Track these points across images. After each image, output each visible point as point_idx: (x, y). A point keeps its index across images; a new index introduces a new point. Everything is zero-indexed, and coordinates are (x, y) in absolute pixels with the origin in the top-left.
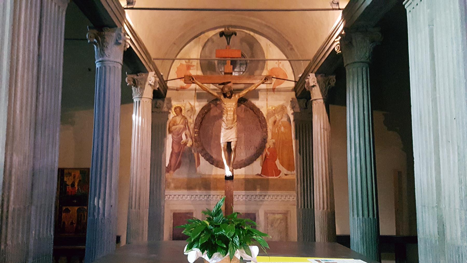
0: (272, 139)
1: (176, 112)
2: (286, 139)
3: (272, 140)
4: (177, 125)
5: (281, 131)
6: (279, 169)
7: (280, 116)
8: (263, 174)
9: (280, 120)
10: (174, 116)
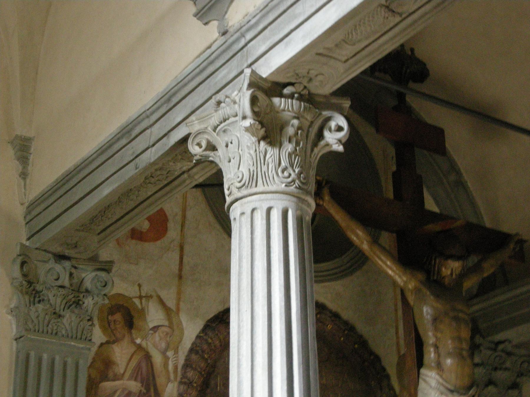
1: (112, 326)
4: (116, 378)
10: (104, 339)
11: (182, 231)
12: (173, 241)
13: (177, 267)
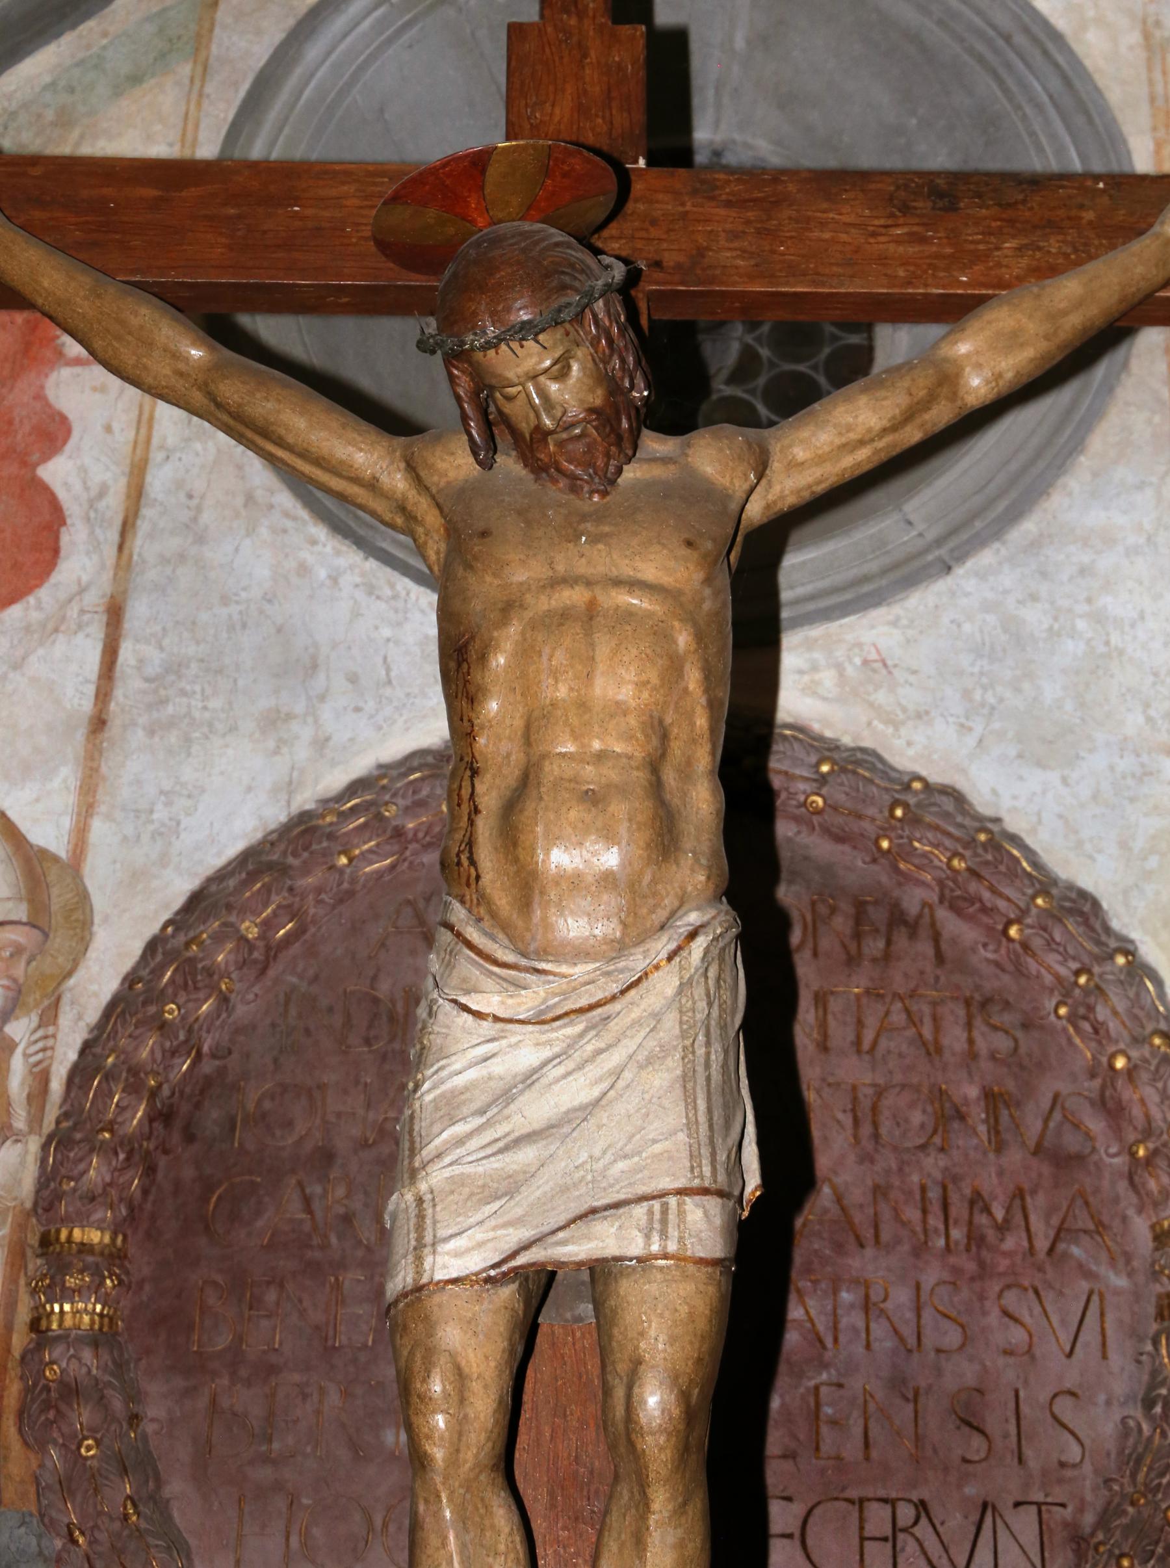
11: (121, 548)
12: (82, 590)
13: (91, 690)
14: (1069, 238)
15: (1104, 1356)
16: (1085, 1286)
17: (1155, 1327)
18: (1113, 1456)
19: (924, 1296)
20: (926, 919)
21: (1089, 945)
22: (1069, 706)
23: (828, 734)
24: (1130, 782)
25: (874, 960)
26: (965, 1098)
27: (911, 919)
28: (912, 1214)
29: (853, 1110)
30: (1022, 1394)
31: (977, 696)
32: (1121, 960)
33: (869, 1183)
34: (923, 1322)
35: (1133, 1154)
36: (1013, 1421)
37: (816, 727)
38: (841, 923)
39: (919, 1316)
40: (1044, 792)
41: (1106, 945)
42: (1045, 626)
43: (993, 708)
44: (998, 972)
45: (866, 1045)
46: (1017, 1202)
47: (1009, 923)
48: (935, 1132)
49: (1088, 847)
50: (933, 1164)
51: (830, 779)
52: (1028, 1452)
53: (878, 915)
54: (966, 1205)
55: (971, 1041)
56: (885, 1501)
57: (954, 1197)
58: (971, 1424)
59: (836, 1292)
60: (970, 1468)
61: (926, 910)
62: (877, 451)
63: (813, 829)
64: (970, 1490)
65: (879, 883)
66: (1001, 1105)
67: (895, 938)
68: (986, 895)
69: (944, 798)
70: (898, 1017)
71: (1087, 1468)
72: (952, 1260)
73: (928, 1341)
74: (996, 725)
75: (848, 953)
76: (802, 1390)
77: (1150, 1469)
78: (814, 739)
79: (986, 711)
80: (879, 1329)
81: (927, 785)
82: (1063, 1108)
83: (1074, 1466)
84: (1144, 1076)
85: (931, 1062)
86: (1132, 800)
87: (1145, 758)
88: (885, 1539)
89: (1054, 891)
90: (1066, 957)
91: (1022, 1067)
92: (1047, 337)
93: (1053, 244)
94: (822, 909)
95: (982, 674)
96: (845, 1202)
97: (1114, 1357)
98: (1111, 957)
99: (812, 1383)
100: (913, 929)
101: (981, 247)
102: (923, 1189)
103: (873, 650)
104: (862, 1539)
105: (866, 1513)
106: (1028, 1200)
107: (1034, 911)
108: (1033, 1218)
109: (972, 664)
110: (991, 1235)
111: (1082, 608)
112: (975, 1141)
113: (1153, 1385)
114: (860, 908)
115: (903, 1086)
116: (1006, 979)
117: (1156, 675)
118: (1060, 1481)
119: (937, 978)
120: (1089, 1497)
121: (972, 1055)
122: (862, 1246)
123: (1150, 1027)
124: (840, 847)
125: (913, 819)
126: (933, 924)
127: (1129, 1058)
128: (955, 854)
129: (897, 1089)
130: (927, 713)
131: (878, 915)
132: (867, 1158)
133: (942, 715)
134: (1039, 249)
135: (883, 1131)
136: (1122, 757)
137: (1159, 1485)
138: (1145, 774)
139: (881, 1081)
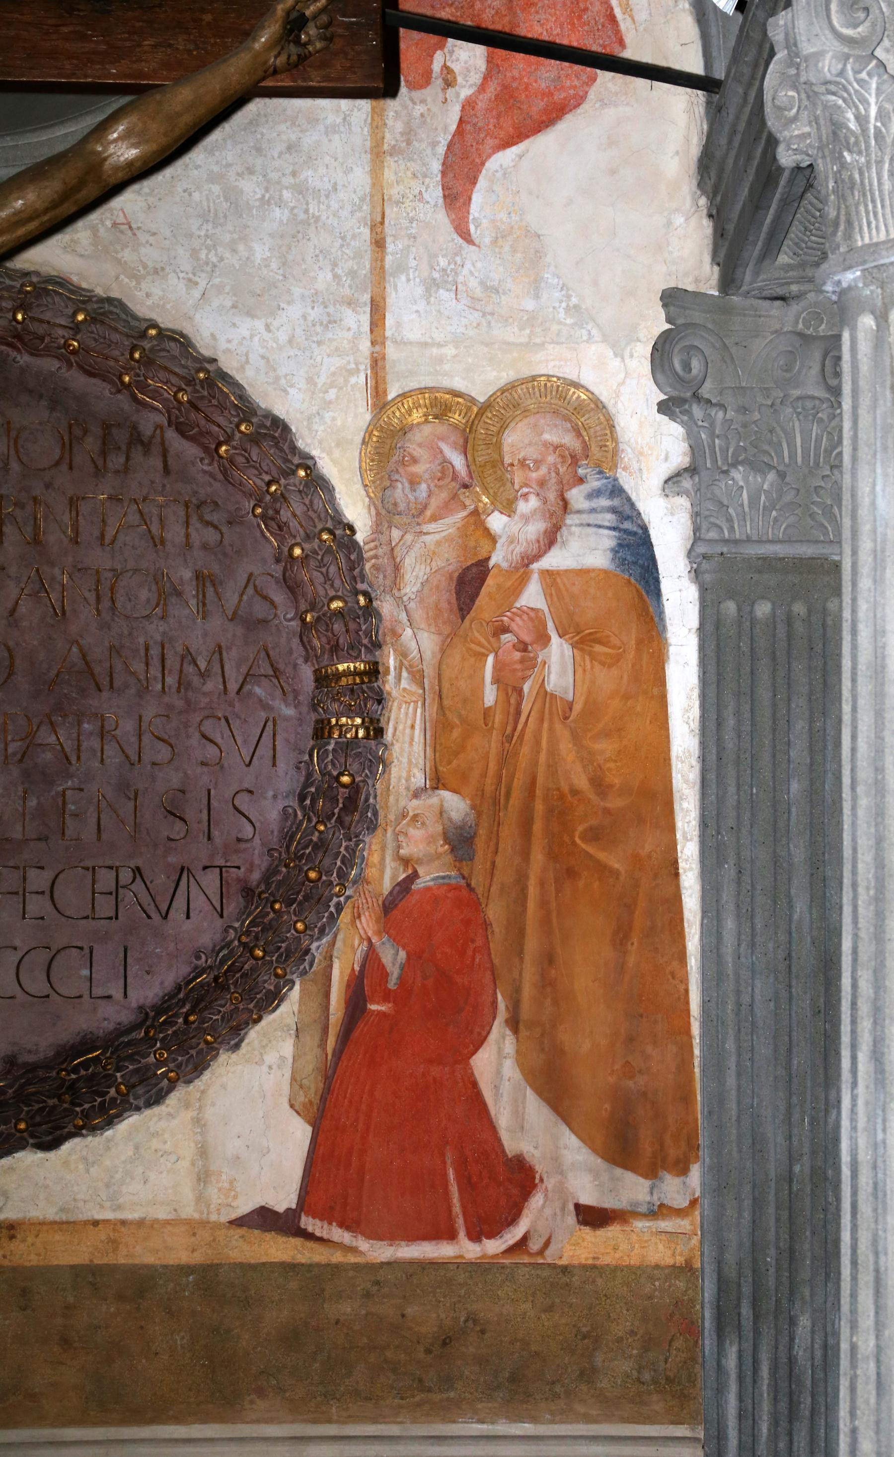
0: (437, 782)
2: (599, 784)
3: (433, 800)
5: (543, 694)
6: (511, 1144)
7: (528, 505)
8: (327, 1215)
9: (529, 559)
14: (192, 37)
15: (274, 765)
16: (263, 715)
17: (312, 743)
18: (276, 833)
19: (144, 725)
20: (158, 439)
21: (279, 462)
22: (274, 266)
23: (84, 285)
24: (318, 329)
25: (117, 472)
26: (181, 578)
27: (145, 439)
28: (138, 666)
29: (97, 590)
30: (212, 792)
31: (203, 256)
32: (302, 473)
33: (107, 644)
34: (143, 744)
35: (303, 621)
36: (205, 812)
37: (75, 279)
38: (91, 444)
39: (140, 740)
40: (252, 336)
41: (291, 462)
42: (259, 196)
43: (215, 266)
44: (212, 480)
45: (107, 540)
46: (217, 656)
47: (219, 444)
48: (157, 605)
49: (283, 381)
50: (155, 630)
51: (82, 327)
52: (215, 833)
53: (121, 436)
54: (178, 659)
55: (187, 536)
56: (111, 868)
57: (169, 654)
58: (174, 814)
59: (79, 724)
60: (173, 844)
61: (158, 431)
62: (42, 224)
63: (72, 365)
64: (172, 859)
65: (122, 410)
66: (208, 584)
67: (133, 455)
68: (203, 422)
69: (172, 344)
70: (133, 518)
71: (257, 841)
72: (166, 699)
73: (146, 758)
74: (217, 281)
75: (96, 467)
76: (53, 793)
77: (299, 843)
78: (72, 292)
79: (209, 269)
80: (111, 750)
81: (160, 330)
82: (255, 586)
83: (247, 841)
84: (313, 563)
85: (156, 552)
86: (319, 343)
87: (331, 309)
88: (111, 893)
89: (254, 420)
90: (260, 471)
91: (225, 555)
92: (165, 135)
93: (180, 43)
94: (77, 432)
95: (207, 236)
96: (88, 658)
97: (281, 765)
98: (294, 473)
99: (60, 789)
100: (147, 447)
101: (128, 44)
102: (147, 649)
103: (121, 214)
104: (94, 893)
105: (97, 876)
106: (224, 654)
107: (238, 435)
108: (227, 668)
109: (200, 229)
110: (196, 681)
111: (288, 180)
112: (187, 611)
113: (306, 785)
114: (107, 428)
115: (136, 571)
116: (217, 485)
117: (343, 238)
118: (237, 851)
119: (164, 486)
120: (257, 862)
121: (188, 545)
122: (100, 690)
123: (320, 526)
124: (93, 380)
125: (148, 361)
126: (163, 443)
127: (303, 550)
128: (180, 389)
129: (131, 573)
130: (163, 269)
131: (121, 436)
132: (105, 626)
133: (175, 271)
134: (170, 46)
135: (118, 605)
136: (313, 308)
137: (304, 854)
138: (330, 322)
139: (119, 567)
